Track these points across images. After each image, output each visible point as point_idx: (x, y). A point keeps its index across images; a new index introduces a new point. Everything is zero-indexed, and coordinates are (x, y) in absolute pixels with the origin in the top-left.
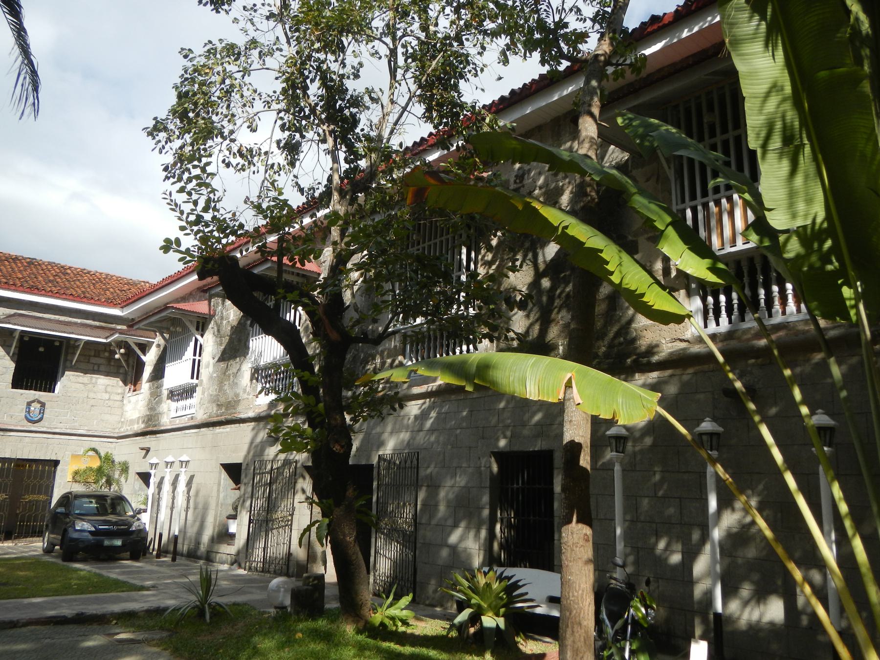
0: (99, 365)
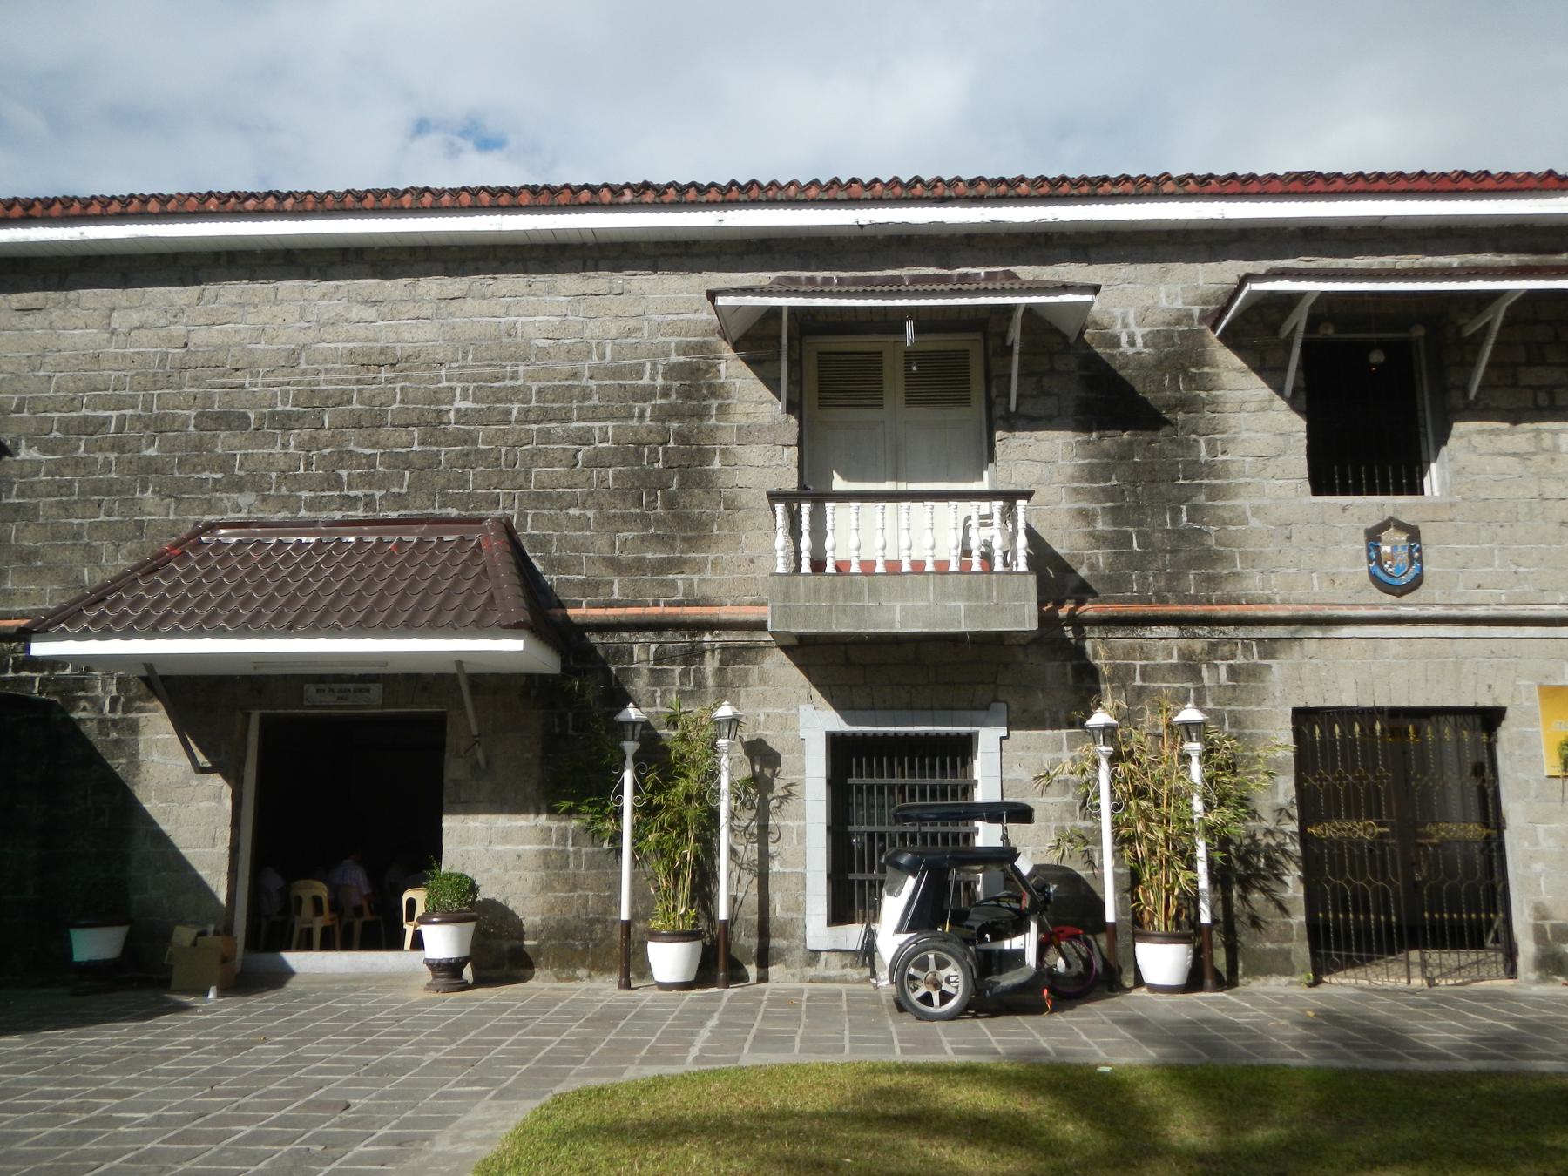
0: (1551, 391)
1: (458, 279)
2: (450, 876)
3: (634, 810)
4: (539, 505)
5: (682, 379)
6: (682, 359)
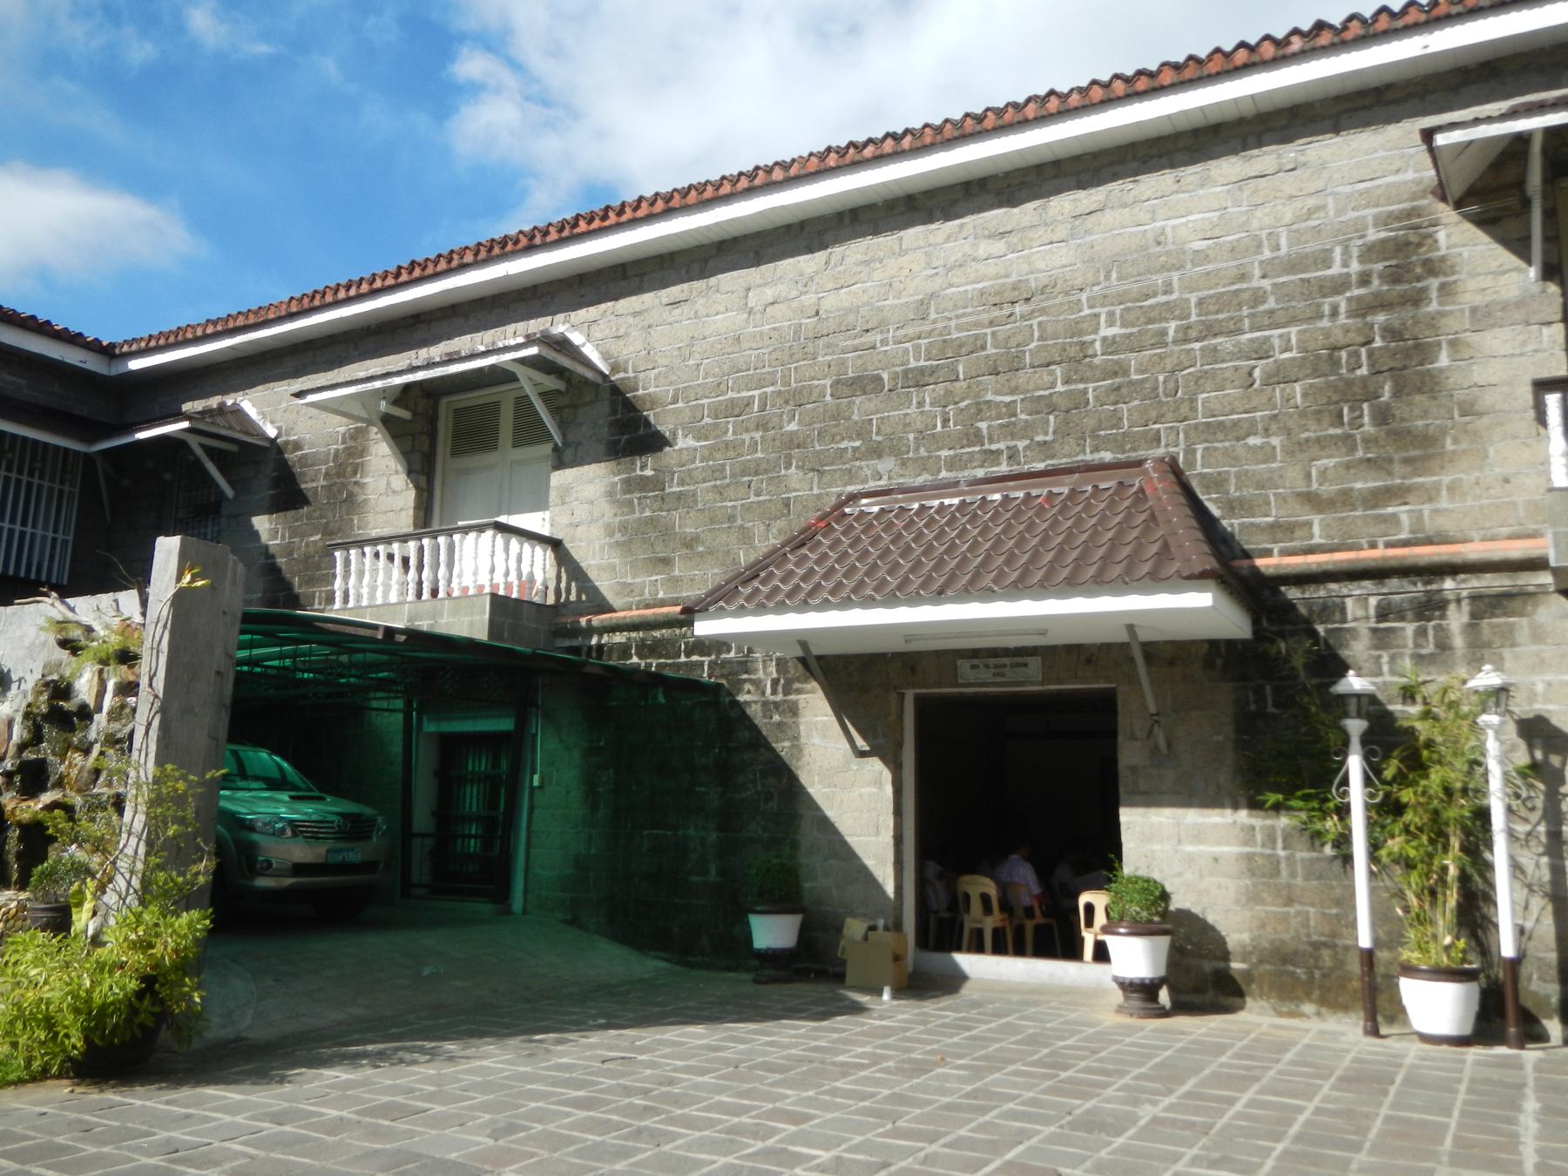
1: (1093, 191)
2: (1134, 880)
3: (1368, 807)
4: (1211, 437)
5: (1386, 259)
6: (1383, 235)
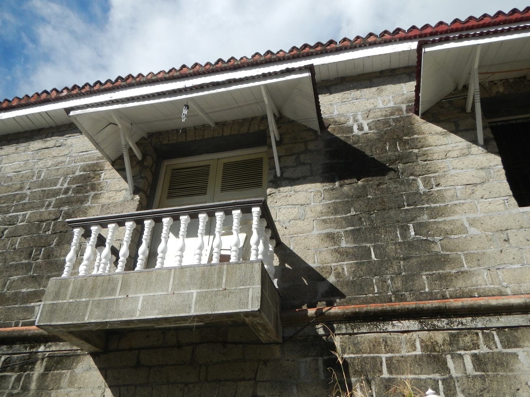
5: (78, 183)
